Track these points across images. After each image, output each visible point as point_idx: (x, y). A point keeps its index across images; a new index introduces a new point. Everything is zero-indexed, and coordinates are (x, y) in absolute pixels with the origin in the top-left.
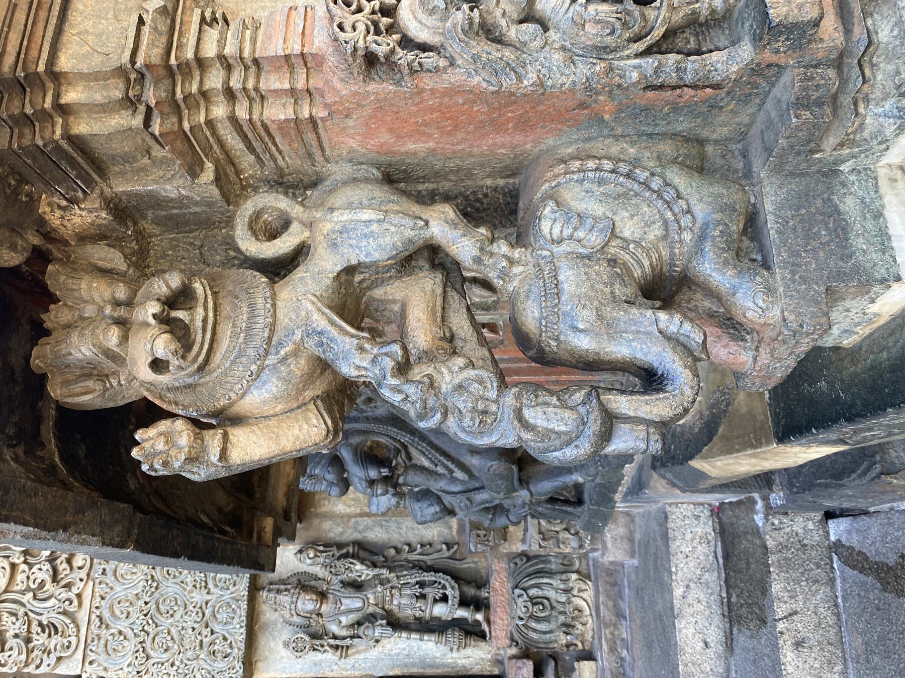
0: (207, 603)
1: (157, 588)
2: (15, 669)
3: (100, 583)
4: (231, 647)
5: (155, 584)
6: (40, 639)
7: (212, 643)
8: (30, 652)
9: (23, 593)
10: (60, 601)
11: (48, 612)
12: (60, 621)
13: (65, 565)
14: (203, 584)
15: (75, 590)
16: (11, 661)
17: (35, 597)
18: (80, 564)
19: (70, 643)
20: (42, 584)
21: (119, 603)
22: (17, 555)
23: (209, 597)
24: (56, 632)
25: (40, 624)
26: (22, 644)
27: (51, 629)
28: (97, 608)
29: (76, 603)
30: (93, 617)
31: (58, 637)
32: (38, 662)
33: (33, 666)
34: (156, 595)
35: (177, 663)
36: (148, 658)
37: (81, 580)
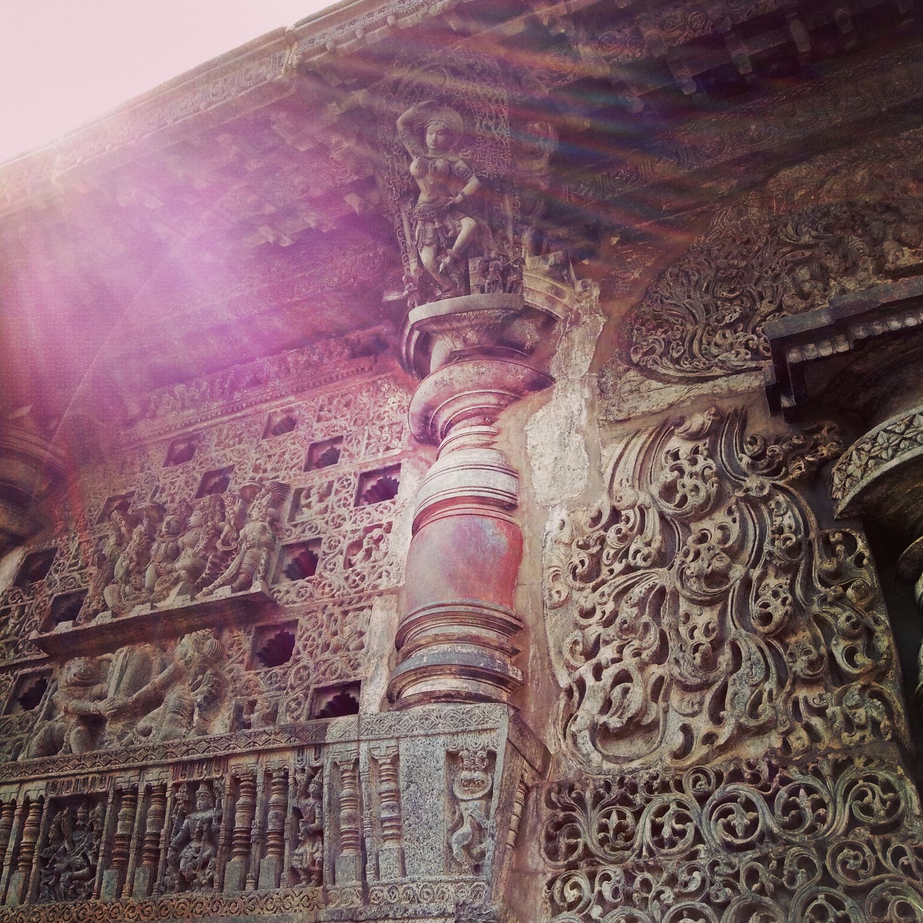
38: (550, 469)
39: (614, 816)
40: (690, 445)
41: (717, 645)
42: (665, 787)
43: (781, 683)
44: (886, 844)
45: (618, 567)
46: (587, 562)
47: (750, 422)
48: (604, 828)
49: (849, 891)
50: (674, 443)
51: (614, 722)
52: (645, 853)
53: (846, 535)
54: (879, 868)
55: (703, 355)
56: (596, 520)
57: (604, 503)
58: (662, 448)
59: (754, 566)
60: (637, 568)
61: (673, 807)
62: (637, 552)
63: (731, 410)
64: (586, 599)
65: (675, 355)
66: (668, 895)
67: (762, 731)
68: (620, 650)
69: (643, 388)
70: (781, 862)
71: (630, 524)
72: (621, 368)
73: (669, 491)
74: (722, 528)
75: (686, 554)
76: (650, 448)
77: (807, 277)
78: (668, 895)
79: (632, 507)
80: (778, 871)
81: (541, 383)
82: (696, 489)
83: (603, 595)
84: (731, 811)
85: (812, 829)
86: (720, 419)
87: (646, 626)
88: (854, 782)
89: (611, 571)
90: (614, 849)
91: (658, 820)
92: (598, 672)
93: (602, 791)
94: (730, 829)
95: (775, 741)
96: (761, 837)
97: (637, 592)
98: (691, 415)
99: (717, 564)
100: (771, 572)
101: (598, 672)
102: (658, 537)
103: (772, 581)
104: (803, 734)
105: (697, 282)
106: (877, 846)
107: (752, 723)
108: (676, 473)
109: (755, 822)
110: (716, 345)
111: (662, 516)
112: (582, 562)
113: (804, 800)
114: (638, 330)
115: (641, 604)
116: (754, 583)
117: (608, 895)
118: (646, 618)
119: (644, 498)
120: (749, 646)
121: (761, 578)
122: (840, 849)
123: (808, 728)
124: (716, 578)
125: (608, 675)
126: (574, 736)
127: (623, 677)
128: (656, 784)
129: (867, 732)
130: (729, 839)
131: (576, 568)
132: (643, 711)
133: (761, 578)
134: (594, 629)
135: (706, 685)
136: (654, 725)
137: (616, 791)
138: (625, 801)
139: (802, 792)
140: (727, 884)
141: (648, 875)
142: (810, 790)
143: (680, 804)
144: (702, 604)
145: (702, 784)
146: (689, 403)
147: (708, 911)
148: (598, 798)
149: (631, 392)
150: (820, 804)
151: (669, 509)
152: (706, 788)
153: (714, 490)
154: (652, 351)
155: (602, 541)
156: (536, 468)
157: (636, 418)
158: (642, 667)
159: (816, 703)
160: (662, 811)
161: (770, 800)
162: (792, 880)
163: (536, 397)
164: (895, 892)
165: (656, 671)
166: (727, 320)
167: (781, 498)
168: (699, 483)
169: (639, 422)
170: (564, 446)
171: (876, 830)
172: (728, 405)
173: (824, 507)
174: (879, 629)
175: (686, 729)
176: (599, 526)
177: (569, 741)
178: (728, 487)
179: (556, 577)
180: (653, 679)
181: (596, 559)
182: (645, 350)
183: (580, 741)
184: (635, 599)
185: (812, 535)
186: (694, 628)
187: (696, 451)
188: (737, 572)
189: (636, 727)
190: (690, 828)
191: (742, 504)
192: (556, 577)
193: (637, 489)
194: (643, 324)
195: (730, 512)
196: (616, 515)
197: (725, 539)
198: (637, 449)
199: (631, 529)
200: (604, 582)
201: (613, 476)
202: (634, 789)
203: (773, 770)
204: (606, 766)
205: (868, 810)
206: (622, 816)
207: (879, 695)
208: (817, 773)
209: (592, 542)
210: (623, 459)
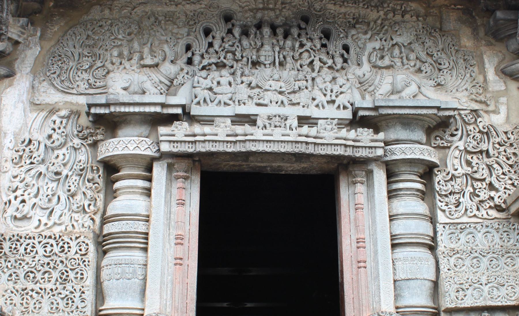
0: (481, 284)
1: (484, 256)
2: (438, 189)
3: (482, 225)
4: (462, 299)
5: (485, 254)
6: (452, 199)
7: (463, 290)
8: (446, 196)
9: (473, 186)
10: (471, 206)
11: (466, 201)
12: (462, 208)
13: (488, 205)
14: (490, 281)
15: (477, 213)
16: (441, 187)
17: (471, 193)
18: (489, 213)
19: (453, 215)
20: (478, 196)
21: (473, 237)
22: (490, 180)
23: (484, 285)
24: (456, 207)
25: (459, 198)
26: (450, 191)
27: (458, 204)
28: (470, 226)
29: (472, 214)
30: (466, 225)
31: (454, 209)
32: (442, 200)
33: (440, 199)
34: (480, 256)
35: (450, 272)
36: (451, 256)
37: (482, 215)
38: (9, 117)
39: (14, 244)
40: (60, 120)
41: (53, 195)
42: (30, 238)
43: (69, 210)
44: (82, 259)
45: (28, 162)
46: (17, 158)
47: (81, 116)
48: (11, 248)
49: (71, 269)
50: (55, 117)
51: (19, 216)
52: (21, 255)
53: (98, 168)
54: (79, 264)
55: (73, 78)
56: (23, 142)
57: (27, 137)
58: (50, 118)
59: (70, 171)
60: (34, 163)
61: (31, 244)
62: (35, 157)
63: (75, 110)
64: (16, 171)
65: (63, 79)
66: (26, 267)
67: (60, 224)
68: (24, 191)
69: (48, 91)
70: (56, 261)
71: (34, 147)
72: (42, 79)
73: (50, 137)
74: (64, 155)
75: (50, 163)
76: (47, 117)
77: (116, 55)
78: (26, 267)
79: (36, 140)
80: (55, 264)
81: (10, 75)
82: (58, 139)
83: (21, 171)
84: (46, 247)
85: (66, 253)
86: (72, 112)
87: (34, 185)
88: (79, 243)
89: (25, 162)
90: (13, 254)
91: (27, 247)
92: (16, 198)
93: (12, 237)
94: (46, 251)
95: (63, 228)
96: (53, 254)
97: (33, 172)
98: (62, 109)
99: (59, 170)
100: (75, 174)
101: (16, 198)
102: (43, 154)
103: (74, 177)
104: (71, 227)
105: (79, 40)
106: (80, 259)
107: (58, 222)
108: (53, 131)
109: (52, 250)
110: (78, 76)
111: (46, 146)
112: (16, 158)
113: (66, 246)
114: (52, 60)
115: (33, 177)
116: (69, 177)
117: (9, 266)
118: (34, 182)
119: (41, 139)
120: (62, 199)
121: (71, 176)
122: (71, 259)
123: (73, 225)
124: (57, 173)
125: (20, 199)
126: (5, 218)
127: (23, 201)
128: (28, 237)
129: (87, 229)
130: (45, 254)
131: (13, 160)
132: (28, 213)
133: (71, 176)
134: (16, 183)
135: (48, 208)
136: (31, 218)
137: (16, 237)
138: (18, 241)
139: (66, 244)
140: (42, 266)
141: (21, 262)
142: (68, 243)
143: (33, 243)
144: (52, 181)
145: (40, 239)
146: (62, 104)
147: (35, 271)
148: (10, 239)
149: (44, 92)
150: (69, 247)
151: (49, 143)
152: (42, 240)
153: (63, 141)
154: (55, 73)
155: (24, 150)
156: (3, 115)
157: (43, 104)
158: (30, 199)
159: (77, 219)
160: (28, 245)
161: (57, 245)
162: (58, 265)
163: (7, 81)
164: (81, 270)
165: (34, 200)
166: (83, 68)
167: (83, 149)
168: (59, 137)
169: (44, 106)
170: (15, 107)
171: (81, 255)
172: (74, 108)
173: (95, 156)
174: (98, 199)
175: (40, 220)
176: (23, 145)
177: (4, 219)
178: (69, 140)
179: (6, 161)
180: (33, 203)
181: (21, 157)
182: (52, 72)
183: (7, 220)
184: (32, 175)
185: (89, 165)
186: (48, 188)
187: (61, 122)
188: (65, 172)
189: (25, 218)
190: (35, 250)
191: (72, 148)
192: (6, 161)
193: (39, 133)
194: (54, 57)
195: (67, 149)
196: (30, 141)
197: (64, 160)
198: (41, 117)
199: (34, 148)
200: (22, 166)
201: (32, 125)
202: (21, 238)
203: (60, 237)
204: (14, 228)
205: (80, 250)
206: (16, 245)
207: (92, 219)
208: (71, 239)
209: (20, 150)
210: (36, 120)
